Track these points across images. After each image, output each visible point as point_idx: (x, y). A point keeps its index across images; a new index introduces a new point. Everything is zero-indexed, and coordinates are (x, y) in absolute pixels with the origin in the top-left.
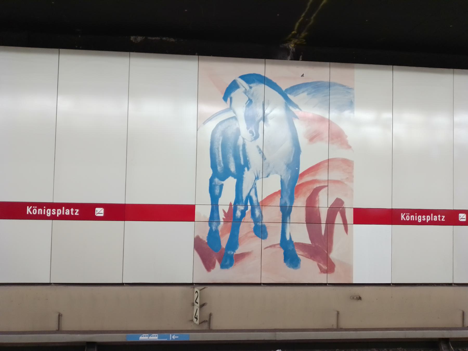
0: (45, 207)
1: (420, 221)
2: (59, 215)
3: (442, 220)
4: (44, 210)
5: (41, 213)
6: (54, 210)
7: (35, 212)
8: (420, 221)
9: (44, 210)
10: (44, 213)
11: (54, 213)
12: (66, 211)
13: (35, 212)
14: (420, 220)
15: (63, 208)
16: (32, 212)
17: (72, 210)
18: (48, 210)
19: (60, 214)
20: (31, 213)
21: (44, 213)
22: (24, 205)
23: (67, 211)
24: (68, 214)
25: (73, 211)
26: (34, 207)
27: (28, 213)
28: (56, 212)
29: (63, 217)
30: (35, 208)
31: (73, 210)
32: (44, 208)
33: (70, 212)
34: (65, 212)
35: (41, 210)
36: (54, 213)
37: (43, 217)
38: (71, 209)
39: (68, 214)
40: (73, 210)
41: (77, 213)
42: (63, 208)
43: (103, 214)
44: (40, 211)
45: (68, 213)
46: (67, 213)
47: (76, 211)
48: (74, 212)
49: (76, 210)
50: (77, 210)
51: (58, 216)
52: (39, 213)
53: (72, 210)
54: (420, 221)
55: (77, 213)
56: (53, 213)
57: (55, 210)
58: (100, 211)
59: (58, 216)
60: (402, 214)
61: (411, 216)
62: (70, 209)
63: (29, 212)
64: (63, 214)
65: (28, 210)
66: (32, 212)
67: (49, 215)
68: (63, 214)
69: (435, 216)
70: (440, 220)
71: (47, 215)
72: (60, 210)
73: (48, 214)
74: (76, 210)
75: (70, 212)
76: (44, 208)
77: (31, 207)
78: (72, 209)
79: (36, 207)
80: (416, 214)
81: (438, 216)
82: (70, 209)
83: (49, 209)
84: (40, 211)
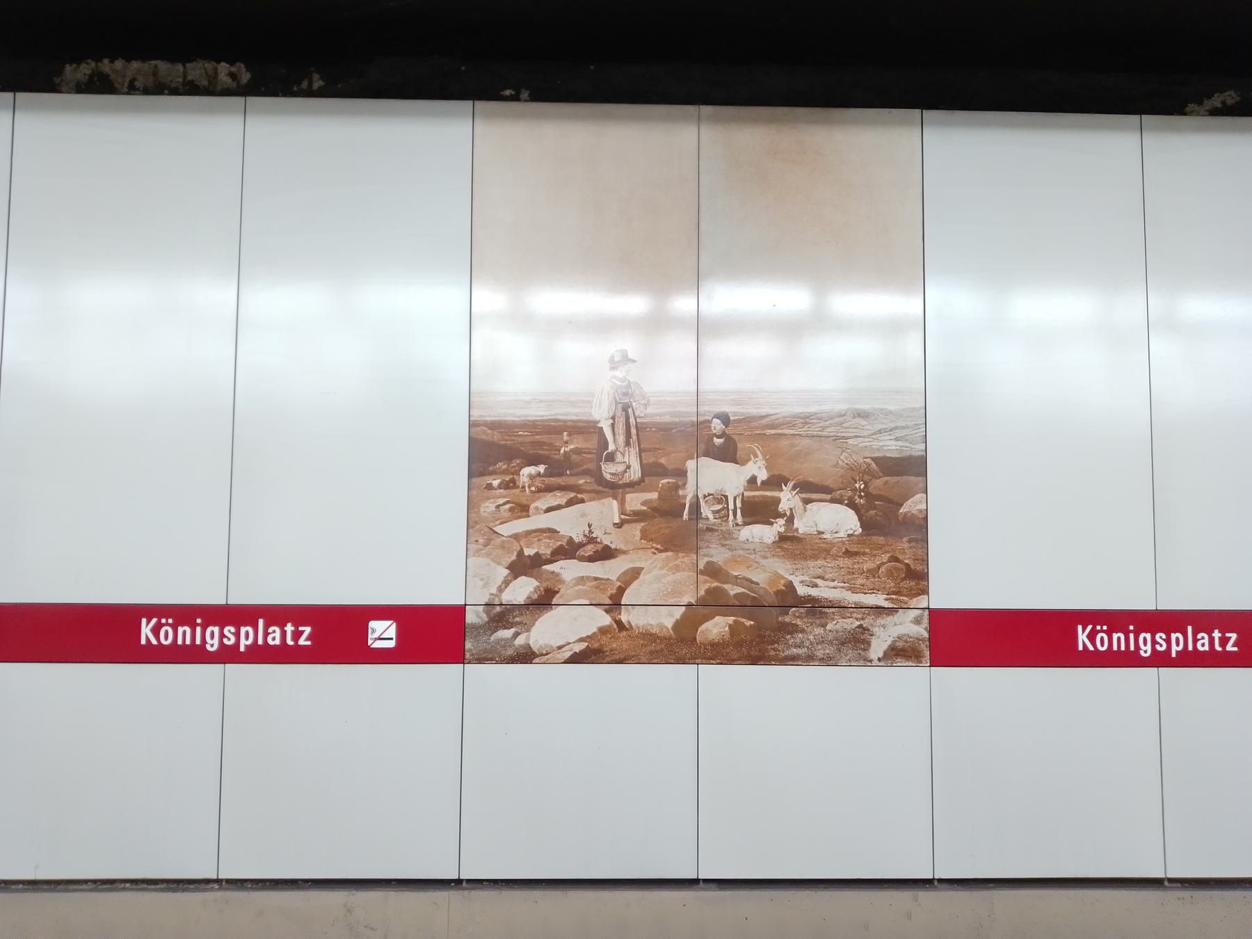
0: (1131, 628)
1: (1146, 651)
2: (1177, 652)
3: (1229, 648)
4: (1132, 636)
5: (188, 642)
6: (229, 631)
7: (1102, 645)
8: (212, 646)
9: (1132, 636)
10: (1132, 648)
11: (1161, 645)
12: (270, 633)
13: (1102, 645)
14: (1149, 648)
15: (1190, 628)
16: (1094, 644)
17: (289, 628)
18: (1142, 635)
19: (1180, 648)
20: (1091, 648)
21: (1132, 648)
22: (1066, 621)
23: (1203, 638)
24: (277, 642)
25: (1220, 638)
26: (1098, 628)
27: (1081, 648)
28: (1168, 641)
29: (1190, 659)
30: (1102, 631)
31: (1220, 635)
32: (1131, 631)
33: (1212, 640)
34: (1195, 641)
35: (1122, 636)
36: (1161, 645)
37: (1129, 659)
38: (1213, 632)
39: (277, 642)
40: (293, 628)
41: (1233, 646)
42: (1190, 628)
43: (394, 639)
44: (1119, 639)
45: (1203, 645)
46: (274, 639)
47: (303, 632)
48: (1224, 641)
49: (1228, 635)
50: (1234, 636)
51: (1174, 655)
52: (1115, 648)
53: (1217, 634)
54: (213, 645)
55: (307, 639)
56: (1158, 647)
57: (1164, 636)
58: (384, 632)
59: (1174, 655)
60: (1080, 627)
61: (180, 629)
62: (282, 626)
63: (1084, 645)
64: (1190, 648)
65: (1082, 637)
66: (1094, 644)
67: (1146, 652)
68: (1190, 648)
69: (1199, 636)
70: (1218, 648)
71: (1142, 653)
72: (250, 629)
73: (211, 642)
74: (1228, 635)
75: (1212, 640)
76: (1131, 631)
77: (1090, 627)
78: (1216, 631)
79: (1105, 628)
80: (199, 621)
81: (1213, 635)
82: (282, 626)
83: (214, 625)
84: (1119, 639)
